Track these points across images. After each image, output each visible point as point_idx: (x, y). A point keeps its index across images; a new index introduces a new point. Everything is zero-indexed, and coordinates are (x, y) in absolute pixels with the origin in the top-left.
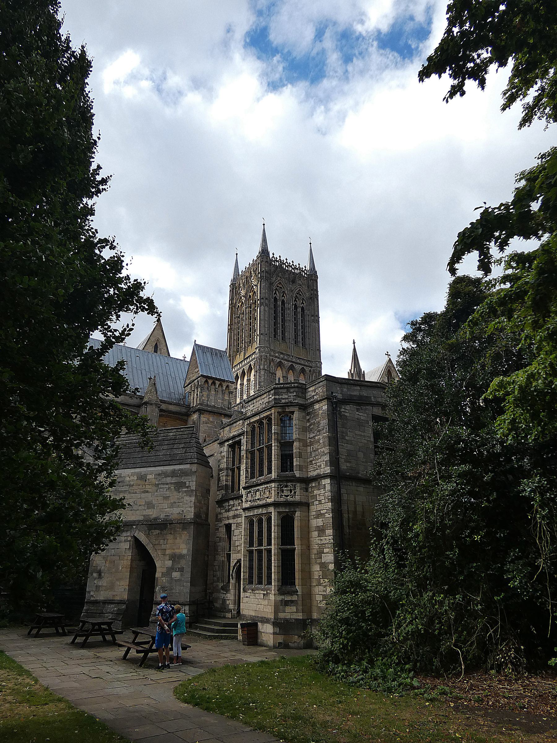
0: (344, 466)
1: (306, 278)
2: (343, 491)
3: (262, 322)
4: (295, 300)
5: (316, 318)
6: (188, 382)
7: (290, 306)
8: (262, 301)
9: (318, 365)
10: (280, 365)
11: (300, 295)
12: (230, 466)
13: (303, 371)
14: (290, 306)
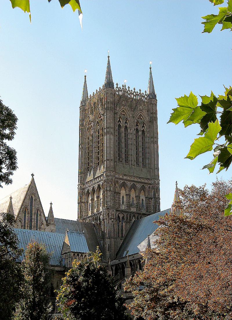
1: (147, 102)
3: (108, 150)
4: (137, 125)
5: (155, 140)
6: (63, 252)
7: (131, 131)
8: (108, 130)
9: (157, 182)
10: (124, 185)
11: (141, 119)
13: (143, 188)
14: (131, 131)
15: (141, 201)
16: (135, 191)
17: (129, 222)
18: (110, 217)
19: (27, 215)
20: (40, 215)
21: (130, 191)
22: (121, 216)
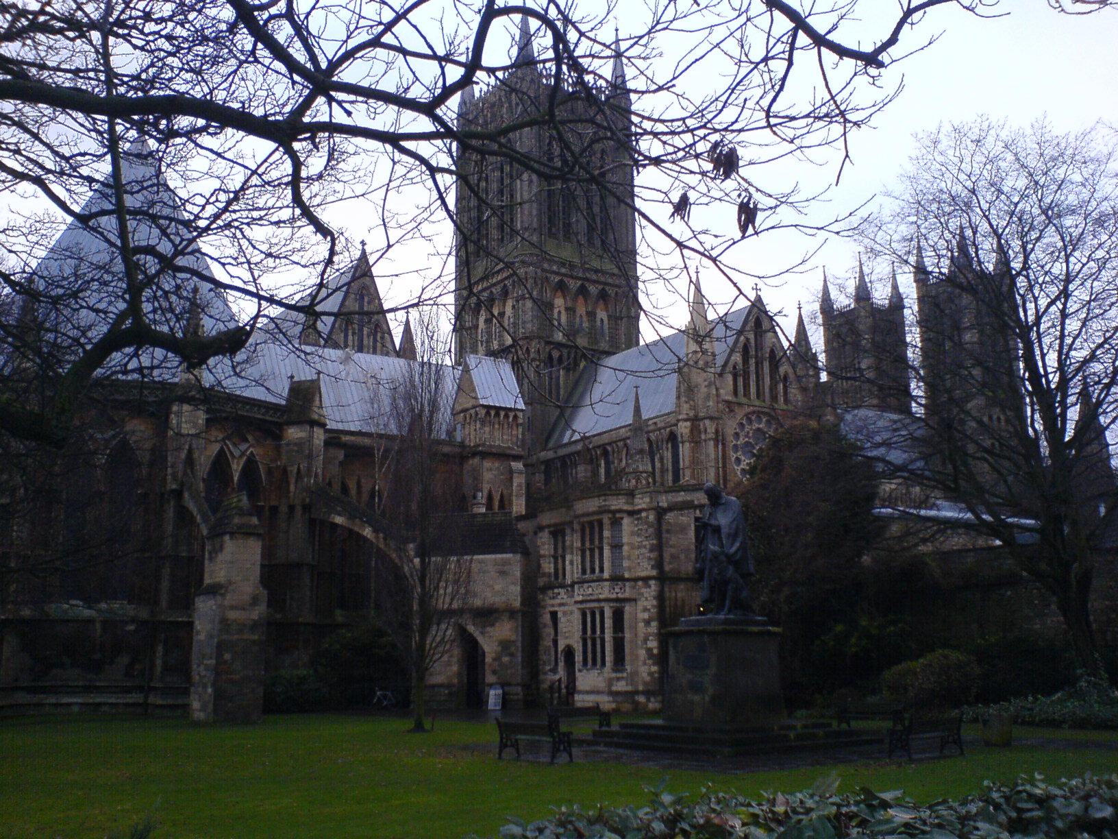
0: (667, 568)
2: (666, 589)
10: (561, 287)
12: (552, 552)
13: (603, 296)
15: (599, 323)
16: (586, 301)
17: (574, 370)
18: (532, 355)
19: (350, 337)
20: (382, 338)
21: (575, 300)
22: (556, 354)
